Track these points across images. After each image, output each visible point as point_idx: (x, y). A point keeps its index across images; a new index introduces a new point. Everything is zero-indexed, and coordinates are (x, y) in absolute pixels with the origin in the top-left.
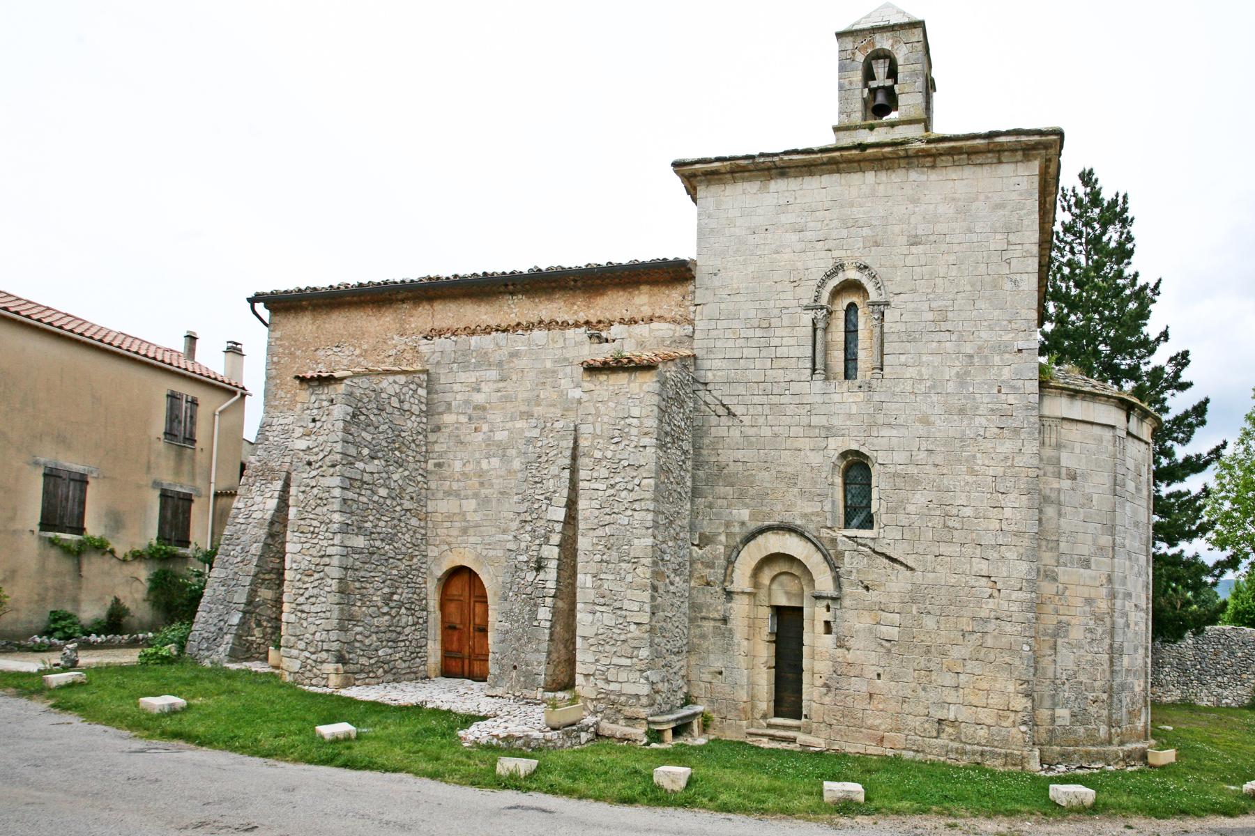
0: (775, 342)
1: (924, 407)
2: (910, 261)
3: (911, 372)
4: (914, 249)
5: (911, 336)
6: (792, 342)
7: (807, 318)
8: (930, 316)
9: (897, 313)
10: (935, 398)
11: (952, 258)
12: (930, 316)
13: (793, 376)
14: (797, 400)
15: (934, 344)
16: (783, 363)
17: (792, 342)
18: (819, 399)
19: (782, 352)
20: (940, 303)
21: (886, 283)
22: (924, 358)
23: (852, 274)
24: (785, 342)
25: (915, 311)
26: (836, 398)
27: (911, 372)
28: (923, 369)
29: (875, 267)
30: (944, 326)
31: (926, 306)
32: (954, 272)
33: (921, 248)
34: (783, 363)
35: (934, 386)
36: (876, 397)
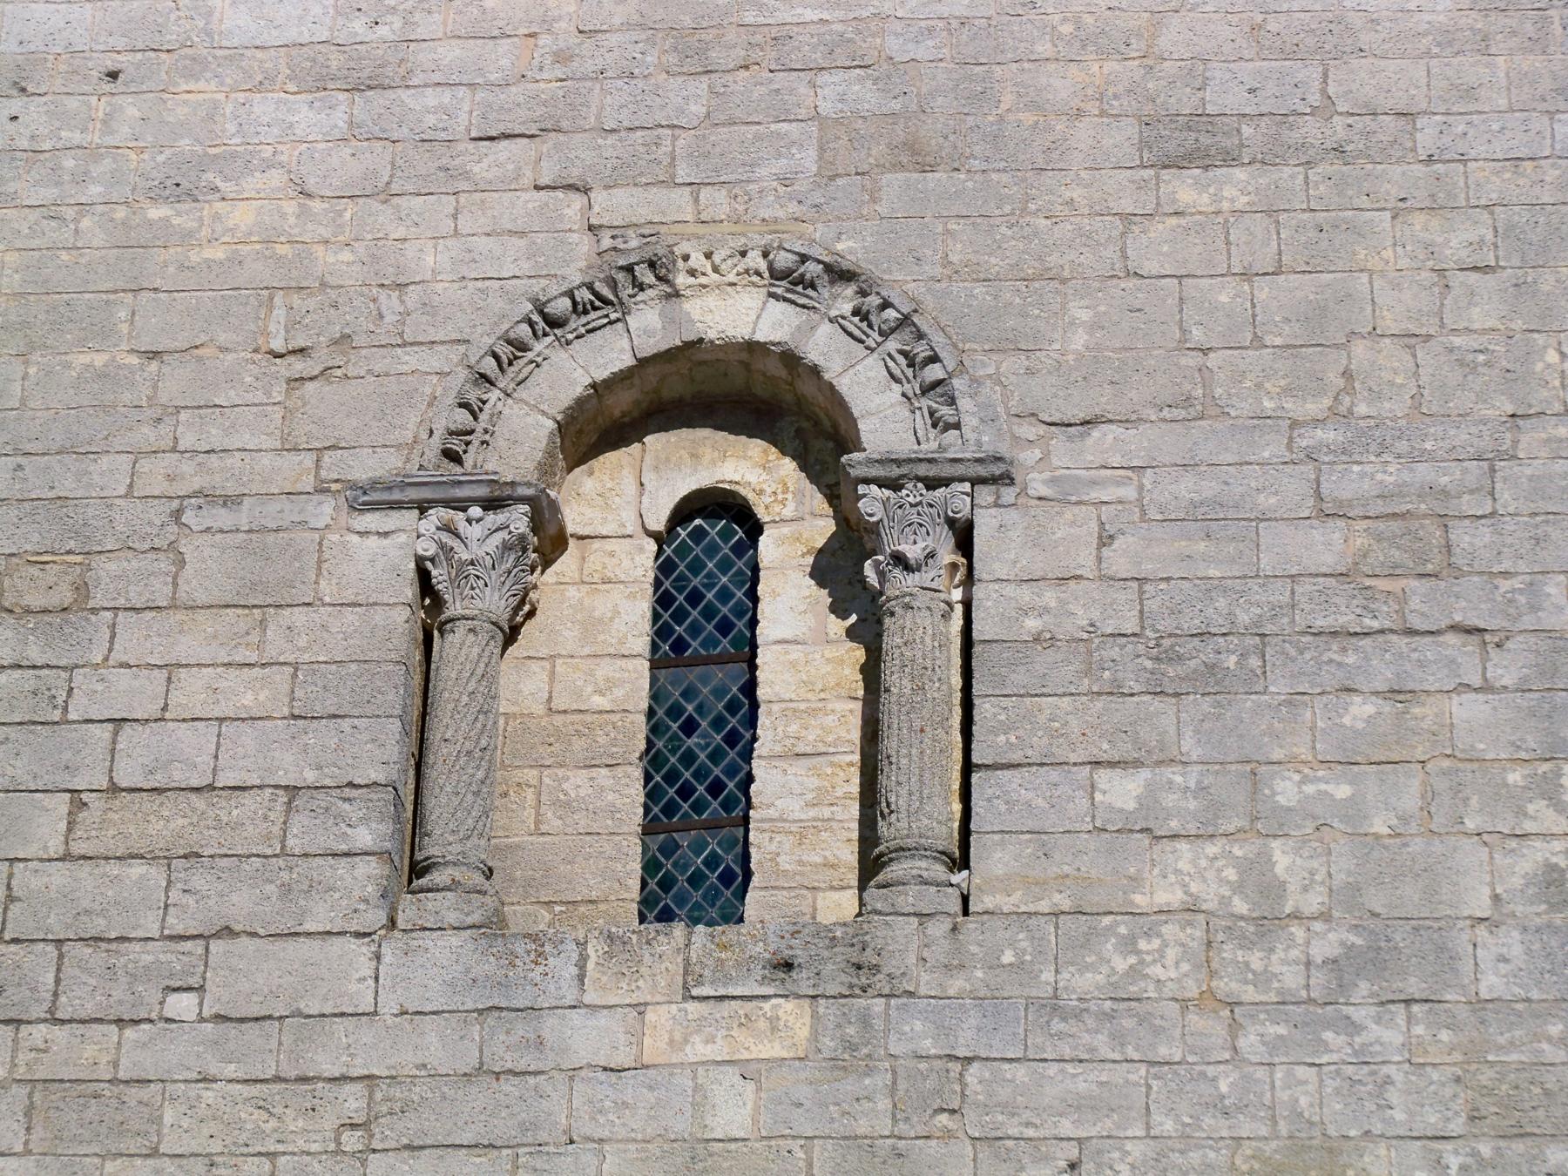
0: (132, 692)
1: (1302, 1090)
2: (1154, 248)
3: (1192, 873)
4: (1185, 189)
5: (1179, 662)
6: (246, 694)
7: (382, 553)
8: (1326, 547)
9: (1072, 534)
10: (1388, 1035)
11: (1460, 239)
12: (1326, 547)
13: (241, 904)
14: (262, 1052)
15: (1360, 710)
16: (166, 824)
17: (246, 694)
18: (438, 1047)
19: (190, 752)
20: (1391, 475)
21: (985, 367)
22: (1286, 790)
23: (734, 313)
24: (191, 692)
25: (1204, 518)
26: (588, 1038)
27: (1192, 873)
28: (1282, 858)
29: (904, 283)
30: (1422, 603)
31: (1293, 488)
32: (1484, 308)
33: (1236, 186)
34: (166, 824)
35: (1369, 959)
36: (914, 1033)
